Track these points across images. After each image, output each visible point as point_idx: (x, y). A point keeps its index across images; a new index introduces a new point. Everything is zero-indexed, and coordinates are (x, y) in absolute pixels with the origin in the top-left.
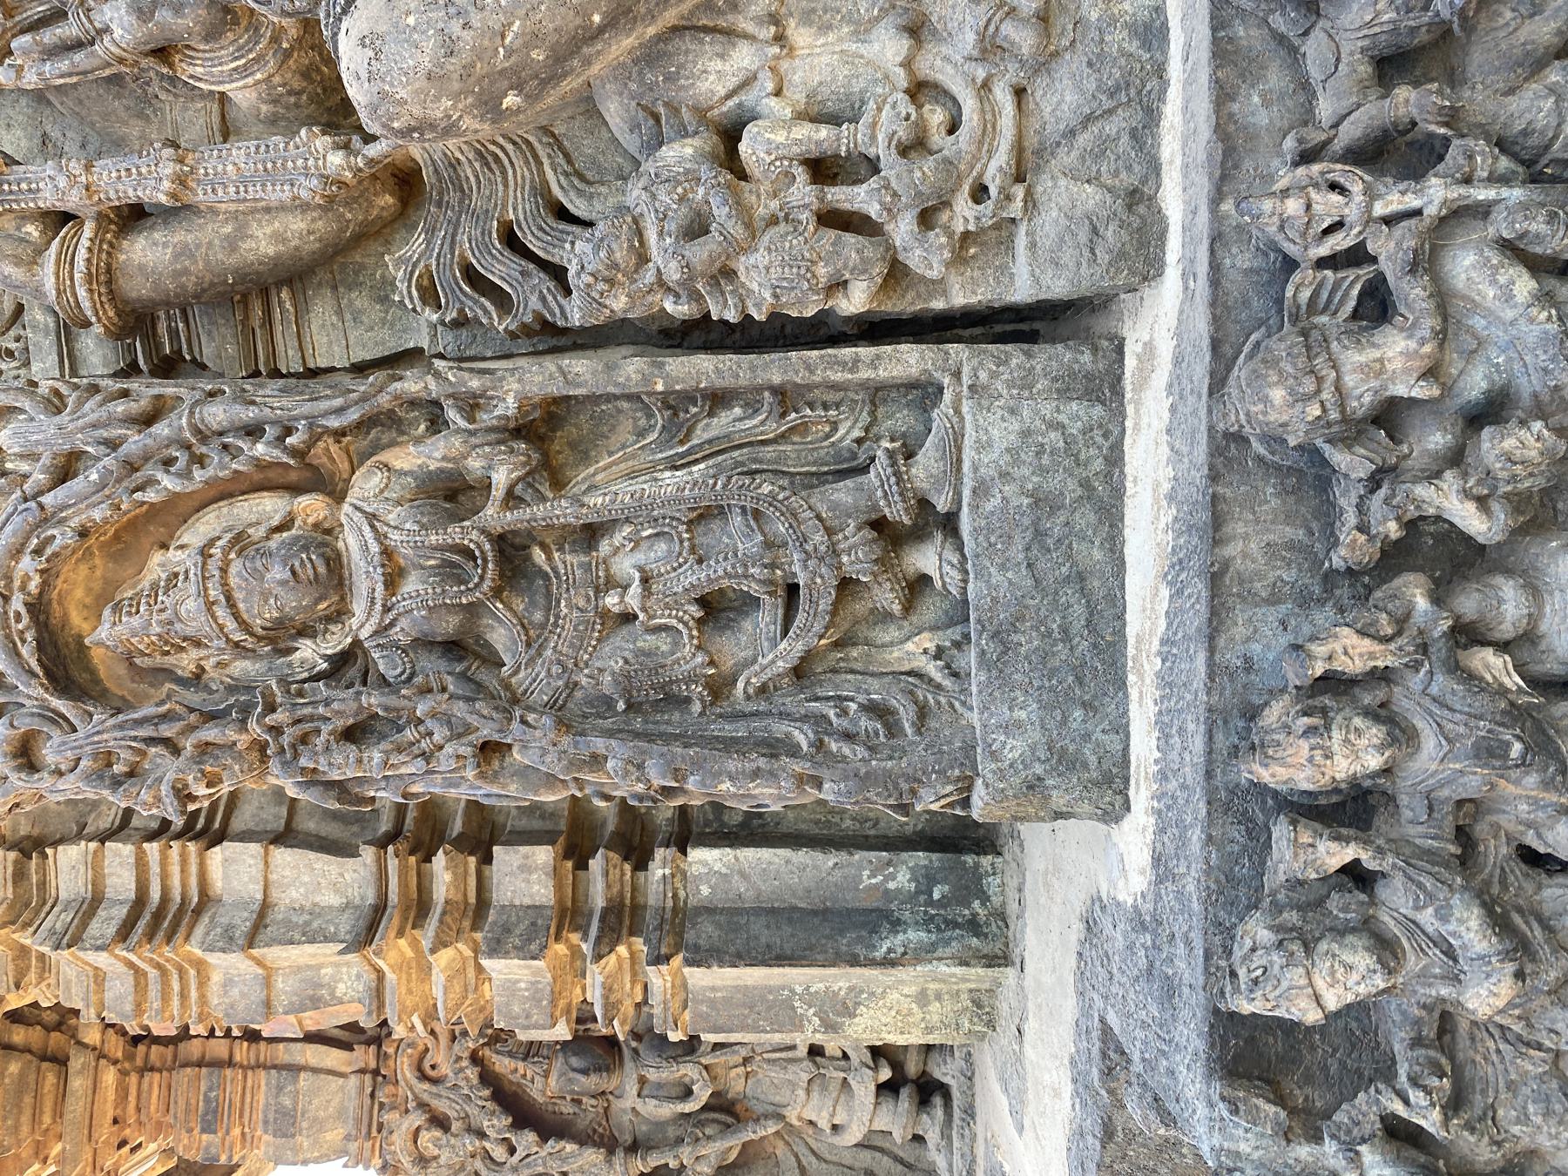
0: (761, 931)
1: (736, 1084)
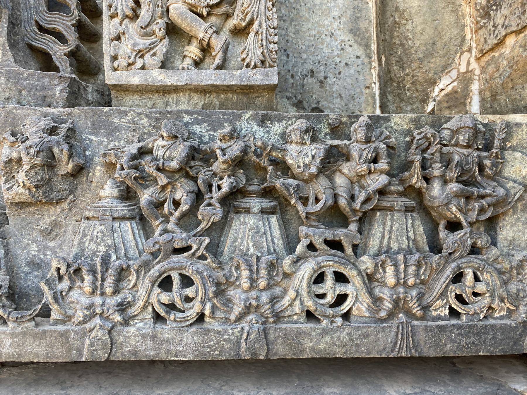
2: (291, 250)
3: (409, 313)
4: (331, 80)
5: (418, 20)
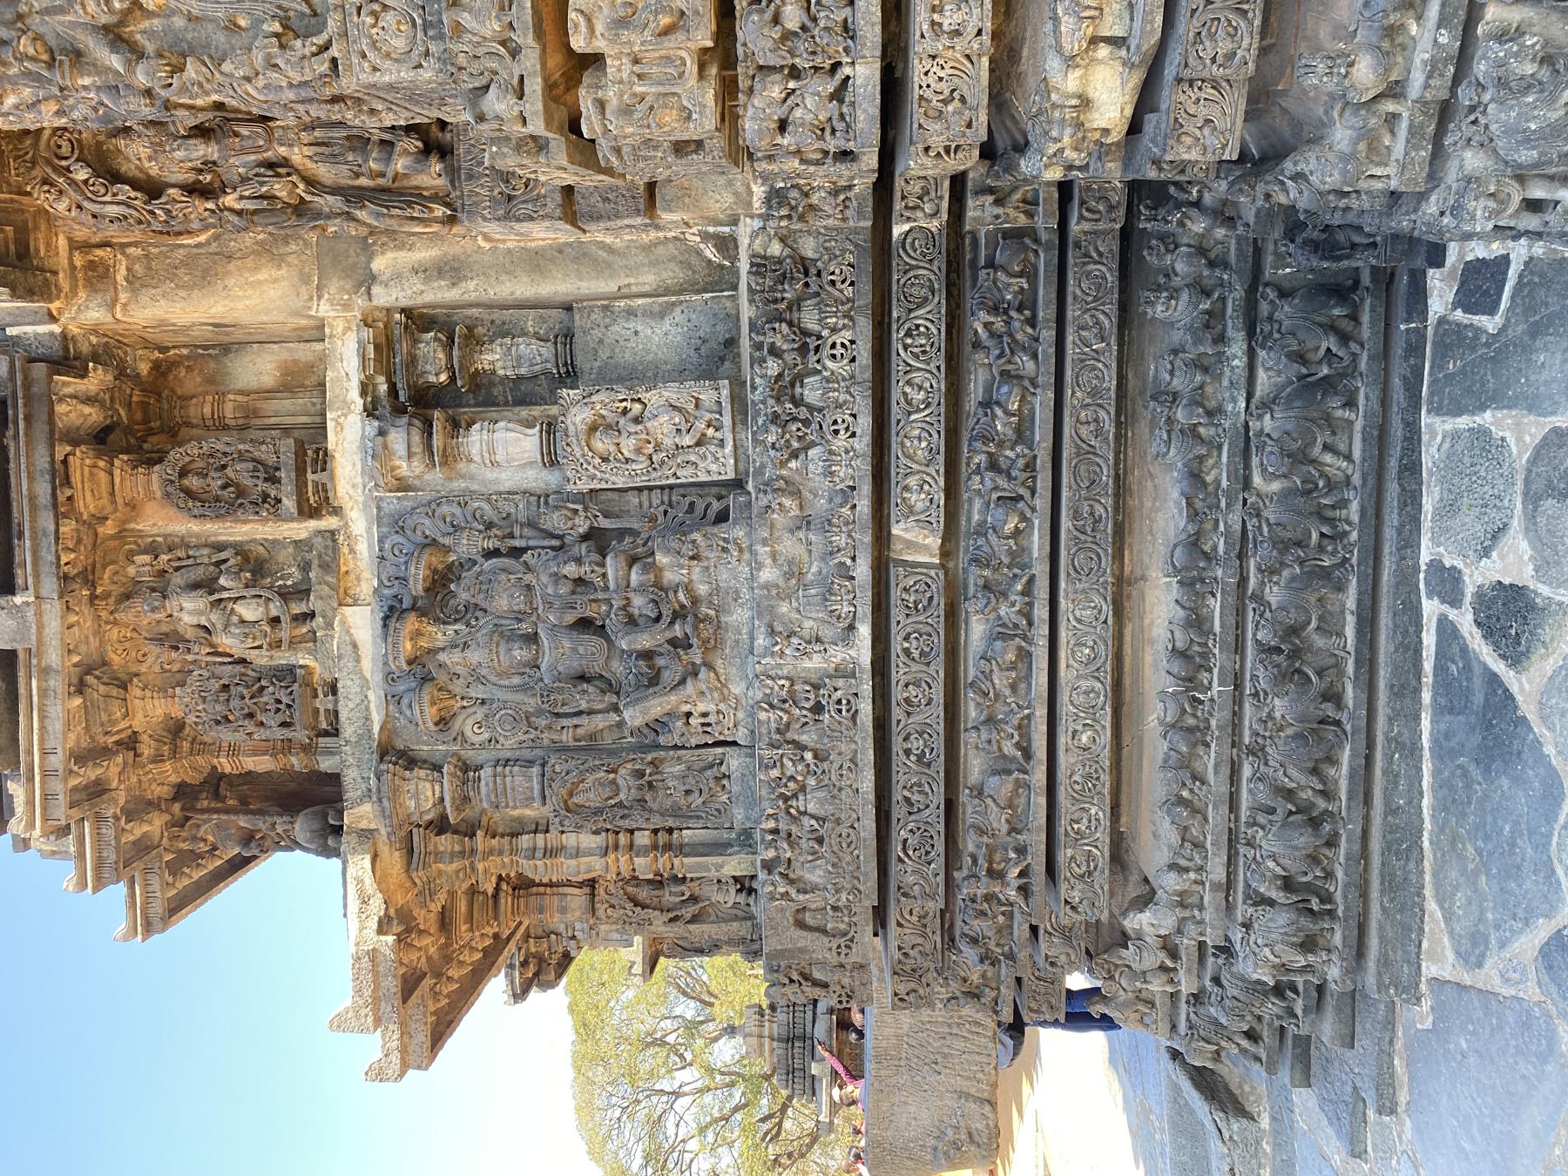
0: (701, 850)
1: (697, 892)
3: (851, 309)
5: (664, 275)
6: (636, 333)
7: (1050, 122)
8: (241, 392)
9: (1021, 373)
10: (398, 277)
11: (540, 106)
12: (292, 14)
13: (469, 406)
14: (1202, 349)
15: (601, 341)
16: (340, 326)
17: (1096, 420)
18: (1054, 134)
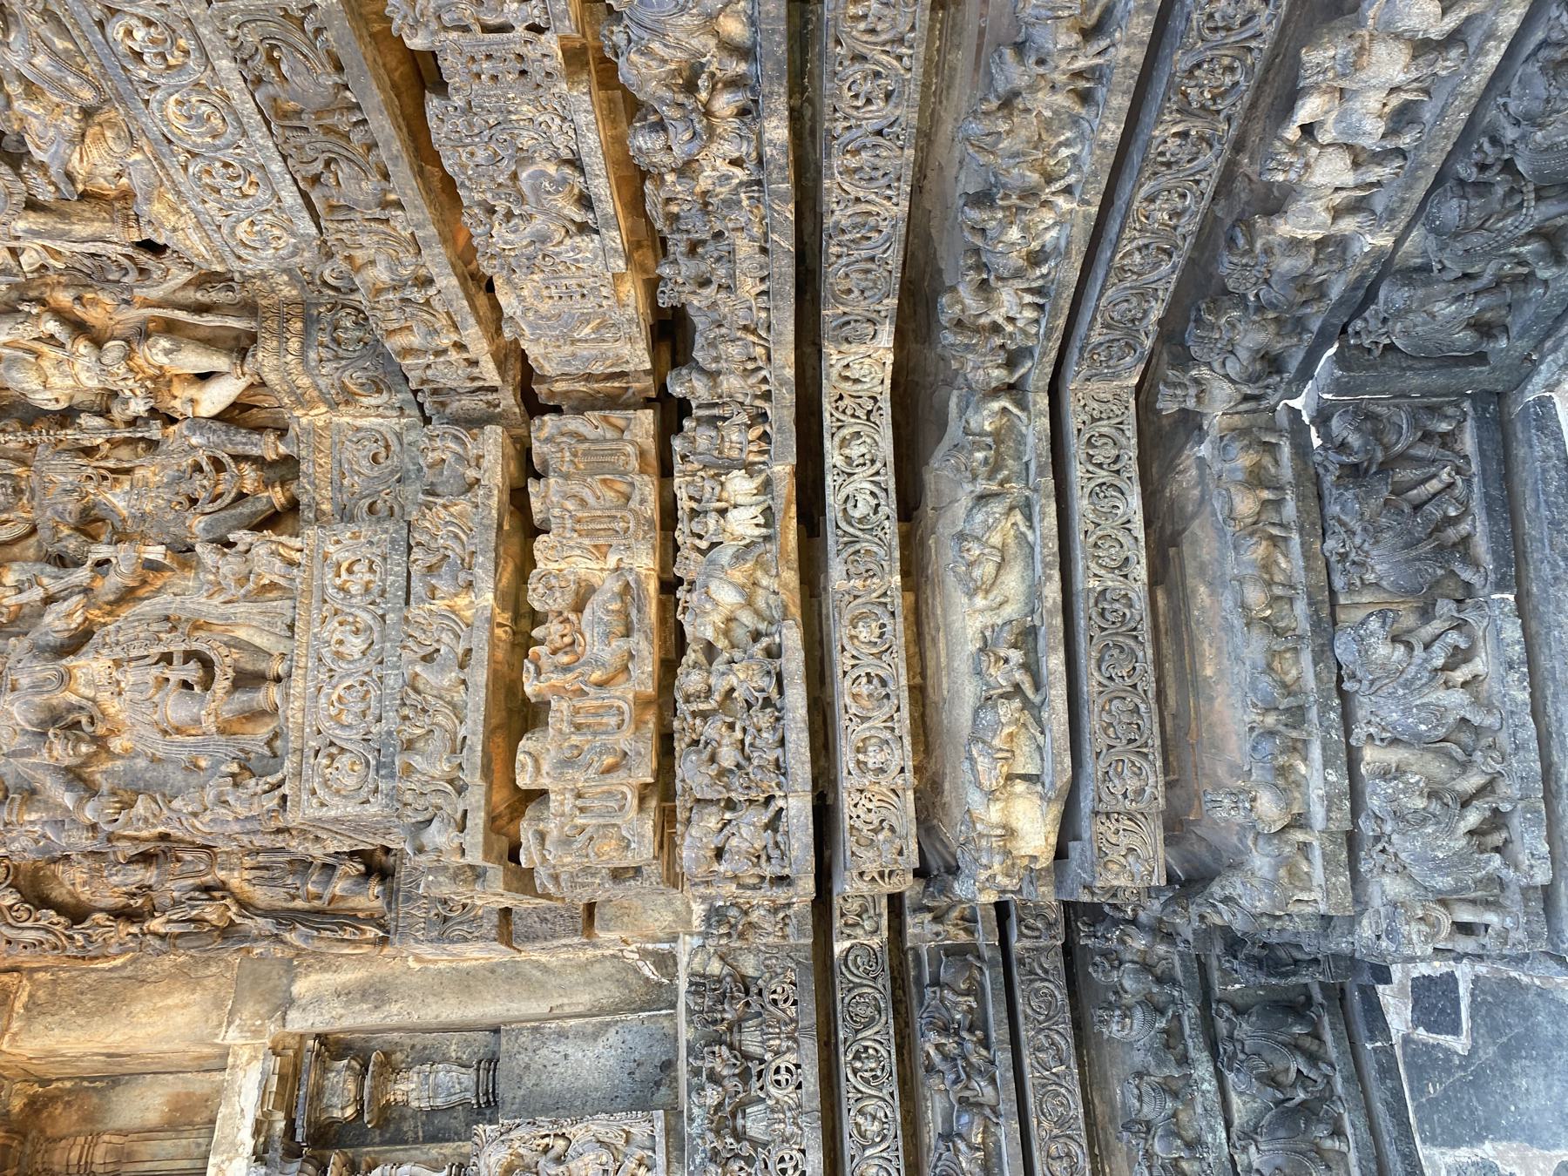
2: (763, 1100)
3: (795, 1030)
4: (636, 1055)
5: (600, 995)
6: (566, 1056)
7: (978, 850)
8: (119, 1132)
9: (981, 1100)
10: (318, 1000)
11: (480, 838)
12: (252, 755)
13: (373, 1144)
14: (1167, 1072)
15: (527, 1067)
16: (246, 1054)
17: (1068, 1155)
18: (984, 861)
